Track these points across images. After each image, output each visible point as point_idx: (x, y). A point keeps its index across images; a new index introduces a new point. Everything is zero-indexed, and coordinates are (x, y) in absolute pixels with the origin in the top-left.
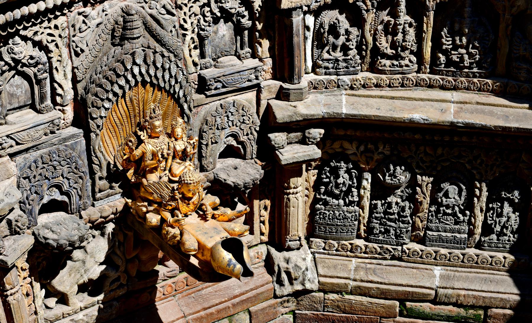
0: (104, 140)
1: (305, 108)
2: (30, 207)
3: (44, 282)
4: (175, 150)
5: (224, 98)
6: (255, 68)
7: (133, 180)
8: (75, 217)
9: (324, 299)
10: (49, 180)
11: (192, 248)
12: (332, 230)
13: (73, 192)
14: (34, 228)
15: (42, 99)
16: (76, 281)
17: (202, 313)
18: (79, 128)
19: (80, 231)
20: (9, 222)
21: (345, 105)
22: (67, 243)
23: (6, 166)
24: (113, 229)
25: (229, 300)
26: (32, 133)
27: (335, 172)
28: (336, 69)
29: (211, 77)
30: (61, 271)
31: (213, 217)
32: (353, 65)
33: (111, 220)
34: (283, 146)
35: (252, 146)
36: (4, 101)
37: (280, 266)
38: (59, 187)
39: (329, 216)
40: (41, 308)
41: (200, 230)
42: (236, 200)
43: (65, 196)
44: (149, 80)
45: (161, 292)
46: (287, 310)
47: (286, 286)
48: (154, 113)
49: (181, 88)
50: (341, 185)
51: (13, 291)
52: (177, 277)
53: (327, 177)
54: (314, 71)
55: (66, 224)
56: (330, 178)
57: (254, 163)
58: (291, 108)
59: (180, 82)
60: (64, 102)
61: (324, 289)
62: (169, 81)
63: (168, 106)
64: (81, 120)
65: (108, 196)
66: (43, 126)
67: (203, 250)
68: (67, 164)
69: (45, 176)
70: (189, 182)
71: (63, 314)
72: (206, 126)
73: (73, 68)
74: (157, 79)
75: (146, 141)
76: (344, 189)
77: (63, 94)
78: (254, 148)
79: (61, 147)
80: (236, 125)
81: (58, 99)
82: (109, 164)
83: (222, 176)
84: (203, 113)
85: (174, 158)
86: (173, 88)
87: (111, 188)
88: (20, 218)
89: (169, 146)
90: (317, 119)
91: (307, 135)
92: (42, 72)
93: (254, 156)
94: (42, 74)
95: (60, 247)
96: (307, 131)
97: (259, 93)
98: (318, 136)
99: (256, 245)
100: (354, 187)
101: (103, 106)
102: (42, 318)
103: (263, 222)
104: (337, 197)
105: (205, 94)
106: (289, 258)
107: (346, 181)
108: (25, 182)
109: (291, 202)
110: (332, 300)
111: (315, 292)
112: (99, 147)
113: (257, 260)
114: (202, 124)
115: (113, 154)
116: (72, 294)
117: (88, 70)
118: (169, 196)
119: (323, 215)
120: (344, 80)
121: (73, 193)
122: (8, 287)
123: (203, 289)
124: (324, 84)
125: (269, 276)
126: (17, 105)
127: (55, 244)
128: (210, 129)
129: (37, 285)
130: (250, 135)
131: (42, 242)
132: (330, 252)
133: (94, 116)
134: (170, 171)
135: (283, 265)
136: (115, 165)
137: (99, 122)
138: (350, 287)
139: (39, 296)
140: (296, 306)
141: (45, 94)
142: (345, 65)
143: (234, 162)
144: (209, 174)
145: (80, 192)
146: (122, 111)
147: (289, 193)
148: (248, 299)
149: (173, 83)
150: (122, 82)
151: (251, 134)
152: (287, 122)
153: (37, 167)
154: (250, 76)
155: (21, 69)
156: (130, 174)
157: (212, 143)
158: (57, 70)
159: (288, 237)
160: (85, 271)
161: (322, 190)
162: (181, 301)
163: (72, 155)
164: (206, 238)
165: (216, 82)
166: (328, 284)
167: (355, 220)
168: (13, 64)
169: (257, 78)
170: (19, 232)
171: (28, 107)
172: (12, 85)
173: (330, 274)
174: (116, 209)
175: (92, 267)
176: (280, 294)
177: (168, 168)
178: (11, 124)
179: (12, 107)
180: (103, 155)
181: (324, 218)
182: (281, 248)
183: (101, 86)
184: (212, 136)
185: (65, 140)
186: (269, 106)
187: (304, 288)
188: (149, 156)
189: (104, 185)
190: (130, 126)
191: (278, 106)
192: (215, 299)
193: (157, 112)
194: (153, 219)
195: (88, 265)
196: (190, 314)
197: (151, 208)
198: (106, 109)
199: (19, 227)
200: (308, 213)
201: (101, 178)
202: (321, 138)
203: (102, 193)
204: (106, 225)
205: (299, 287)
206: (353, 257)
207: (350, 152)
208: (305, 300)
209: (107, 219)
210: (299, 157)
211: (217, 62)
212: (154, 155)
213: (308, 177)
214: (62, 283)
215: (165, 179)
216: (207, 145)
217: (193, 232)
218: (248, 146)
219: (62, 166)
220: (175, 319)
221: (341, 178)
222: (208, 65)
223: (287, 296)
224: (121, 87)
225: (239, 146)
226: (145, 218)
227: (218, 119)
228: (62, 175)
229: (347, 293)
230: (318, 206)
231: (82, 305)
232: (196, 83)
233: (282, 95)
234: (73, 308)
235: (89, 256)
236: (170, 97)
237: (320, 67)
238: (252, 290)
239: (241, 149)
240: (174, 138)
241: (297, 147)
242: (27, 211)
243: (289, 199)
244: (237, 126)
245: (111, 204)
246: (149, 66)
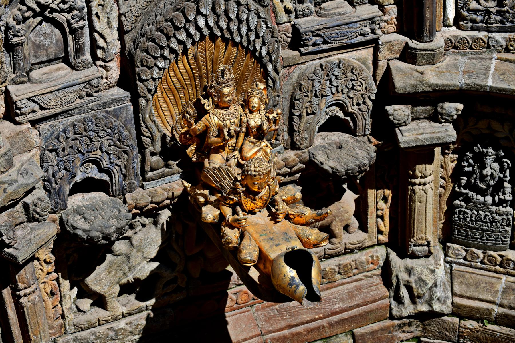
0: (159, 106)
1: (437, 75)
2: (57, 187)
3: (75, 279)
4: (248, 127)
5: (326, 57)
6: (371, 19)
7: (194, 159)
8: (119, 201)
9: (460, 326)
10: (83, 154)
11: (248, 258)
12: (475, 235)
13: (115, 170)
14: (61, 212)
15: (79, 51)
16: (117, 279)
17: (286, 332)
18: (126, 89)
19: (120, 221)
20: (26, 206)
21: (493, 75)
22: (101, 235)
23: (25, 137)
24: (169, 217)
25: (324, 318)
26: (62, 96)
27: (480, 160)
28: (486, 23)
29: (307, 29)
30: (97, 267)
31: (287, 217)
32: (511, 19)
33: (167, 206)
34: (405, 122)
35: (365, 119)
36: (27, 54)
37: (400, 277)
38: (96, 163)
39: (471, 215)
40: (70, 312)
41: (265, 235)
42: (345, 186)
43: (104, 174)
44: (219, 34)
45: (233, 300)
46: (409, 336)
47: (406, 305)
48: (223, 77)
49: (264, 44)
50: (489, 178)
51: (27, 291)
53: (469, 165)
54: (456, 23)
55: (103, 210)
56: (473, 167)
57: (367, 142)
58: (417, 74)
59: (262, 37)
60: (106, 56)
61: (459, 312)
62: (247, 35)
63: (247, 65)
64: (128, 80)
65: (163, 176)
66: (76, 88)
67: (265, 261)
68: (108, 135)
69: (78, 149)
70: (254, 173)
71: (99, 321)
72: (299, 92)
73: (120, 15)
74: (231, 33)
75: (211, 112)
76: (492, 183)
77: (105, 47)
78: (367, 122)
79: (101, 114)
80: (342, 91)
81: (100, 53)
82: (164, 136)
83: (320, 158)
84: (296, 75)
85: (247, 135)
86: (252, 43)
87: (167, 166)
88: (39, 202)
89: (241, 119)
90: (452, 90)
91: (439, 109)
92: (77, 19)
93: (367, 133)
94: (77, 22)
95: (91, 240)
96: (440, 105)
97: (376, 50)
98: (455, 112)
99: (372, 246)
100: (506, 181)
101: (156, 65)
102: (71, 323)
103: (382, 217)
104: (483, 193)
105: (300, 51)
106: (412, 268)
107: (495, 173)
108: (51, 156)
109: (417, 195)
110: (469, 329)
111: (447, 315)
112: (151, 115)
113: (371, 266)
114: (295, 89)
115: (171, 124)
116: (112, 296)
117: (139, 19)
118: (231, 187)
119: (463, 214)
120: (497, 39)
121: (115, 171)
122: (21, 285)
124: (468, 43)
125: (385, 289)
126: (45, 58)
127: (85, 237)
128: (305, 96)
129: (66, 284)
130: (362, 105)
131: (69, 232)
132: (472, 263)
133: (144, 77)
134: (241, 151)
135: (404, 276)
136: (173, 137)
137: (152, 85)
138: (494, 314)
139: (68, 296)
140: (421, 331)
141: (81, 47)
142: (499, 18)
143: (341, 138)
144: (303, 153)
145: (124, 170)
146: (183, 72)
147: (414, 184)
148: (351, 317)
149: (253, 38)
150: (183, 36)
151: (364, 103)
152: (409, 93)
153: (67, 138)
154: (364, 29)
155: (50, 16)
156: (191, 150)
157: (308, 114)
158: (98, 17)
159: (412, 240)
160: (130, 269)
161: (463, 182)
162: (259, 313)
163: (115, 124)
164: (271, 246)
165: (314, 36)
166: (465, 306)
167: (508, 225)
168: (38, 10)
169: (373, 31)
170: (38, 218)
171: (61, 60)
172: (38, 34)
173: (468, 294)
174: (173, 193)
175: (139, 264)
176: (398, 314)
177: (238, 148)
178: (36, 83)
179: (38, 61)
180: (157, 126)
181: (465, 219)
182: (403, 254)
183: (153, 40)
184: (308, 104)
186: (388, 70)
187: (430, 309)
188: (214, 131)
189: (158, 162)
190: (194, 90)
191: (399, 70)
192: (306, 313)
193: (227, 76)
194: (210, 213)
195: (133, 261)
196: (269, 332)
197: (213, 198)
198: (160, 69)
199: (38, 213)
200: (445, 210)
201: (153, 154)
202: (458, 115)
203: (155, 172)
204: (160, 212)
205: (424, 308)
206: (504, 274)
207: (501, 135)
208: (434, 326)
209: (161, 205)
210: (425, 139)
211: (320, 8)
212: (220, 130)
213: (445, 163)
214: (98, 281)
215: (233, 162)
216: (300, 116)
217: (256, 236)
218: (360, 119)
219: (101, 138)
220: (248, 337)
221: (488, 169)
222: (307, 12)
223: (408, 317)
224: (180, 42)
225: (346, 118)
226: (201, 213)
227: (317, 84)
228: (101, 149)
229: (490, 322)
230: (457, 202)
231: (125, 310)
232: (290, 35)
233: (408, 55)
234: (113, 313)
235: (135, 250)
236: (249, 55)
237: (464, 19)
238: (358, 306)
239: (350, 122)
240: (249, 109)
241: (425, 124)
242: (53, 191)
243: (413, 191)
244: (343, 94)
245: (166, 186)
246: (218, 16)
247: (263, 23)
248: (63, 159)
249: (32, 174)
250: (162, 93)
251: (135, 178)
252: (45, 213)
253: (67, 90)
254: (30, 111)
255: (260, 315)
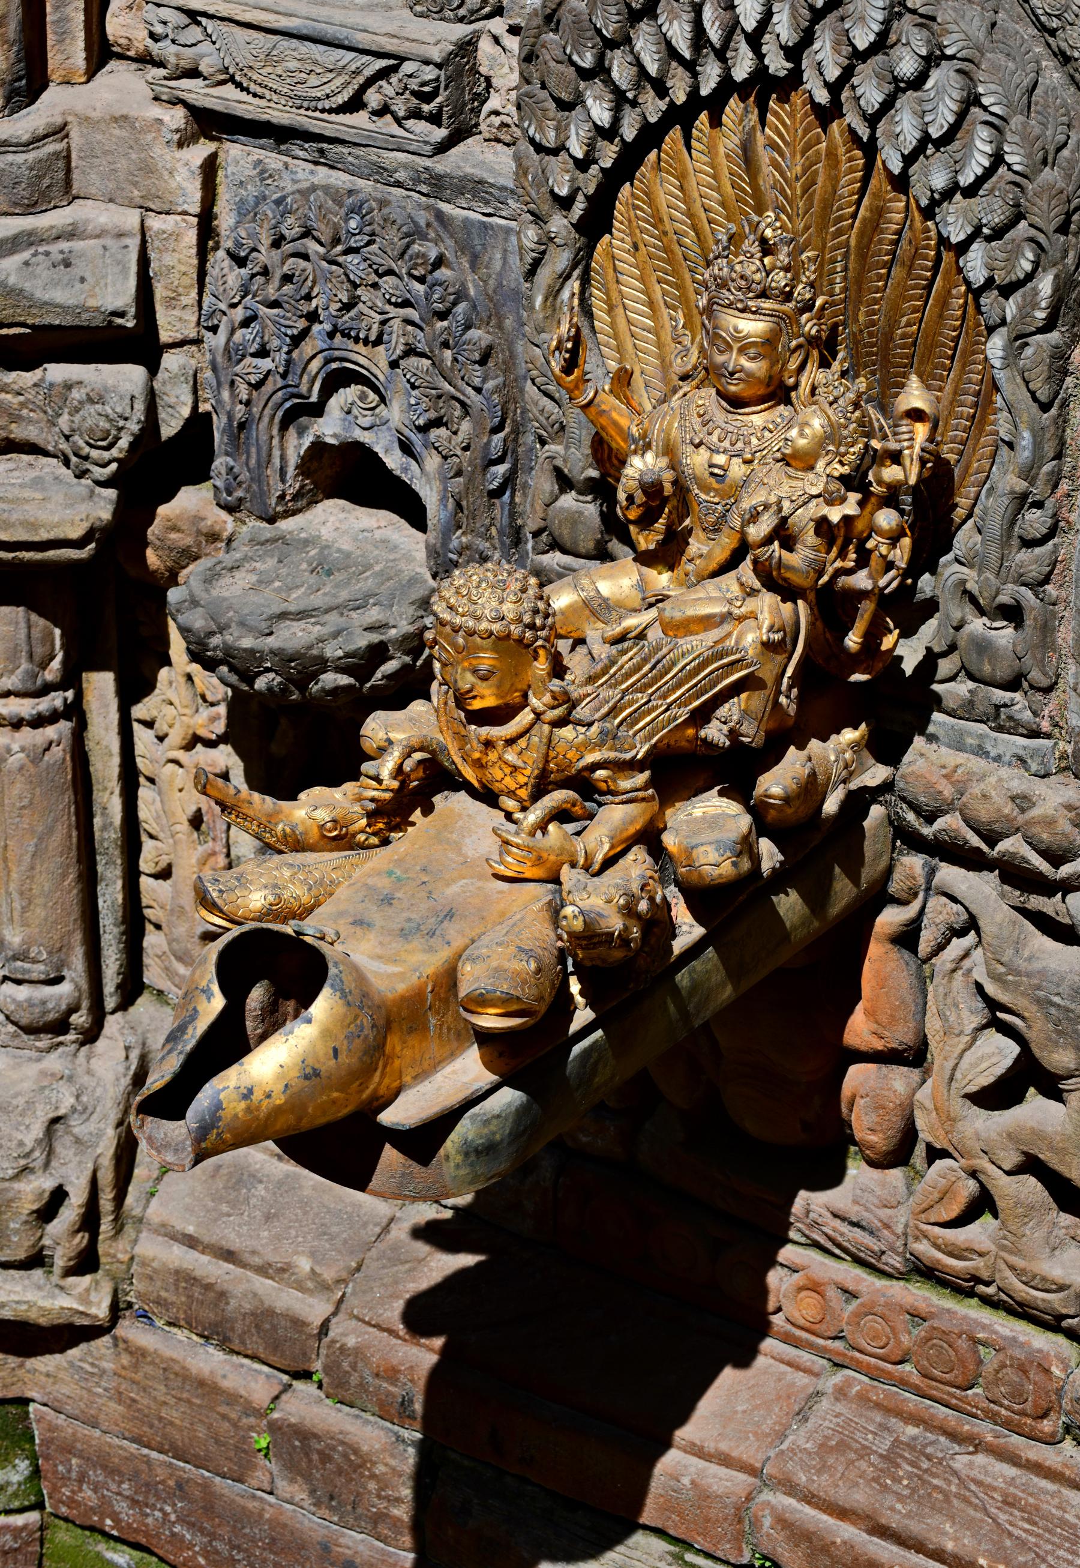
22: (215, 641)
23: (145, 148)
26: (293, 65)
44: (822, 96)
52: (881, 1283)
68: (406, 304)
108: (235, 277)
123: (977, 1445)
162: (839, 1408)
185: (439, 186)
189: (574, 519)
192: (970, 1524)
196: (790, 1488)
220: (710, 1446)
247: (984, 132)
248: (263, 311)
249: (83, 280)
250: (636, 247)
251: (502, 543)
252: (95, 454)
253: (316, 51)
254: (185, 64)
255: (827, 1414)
